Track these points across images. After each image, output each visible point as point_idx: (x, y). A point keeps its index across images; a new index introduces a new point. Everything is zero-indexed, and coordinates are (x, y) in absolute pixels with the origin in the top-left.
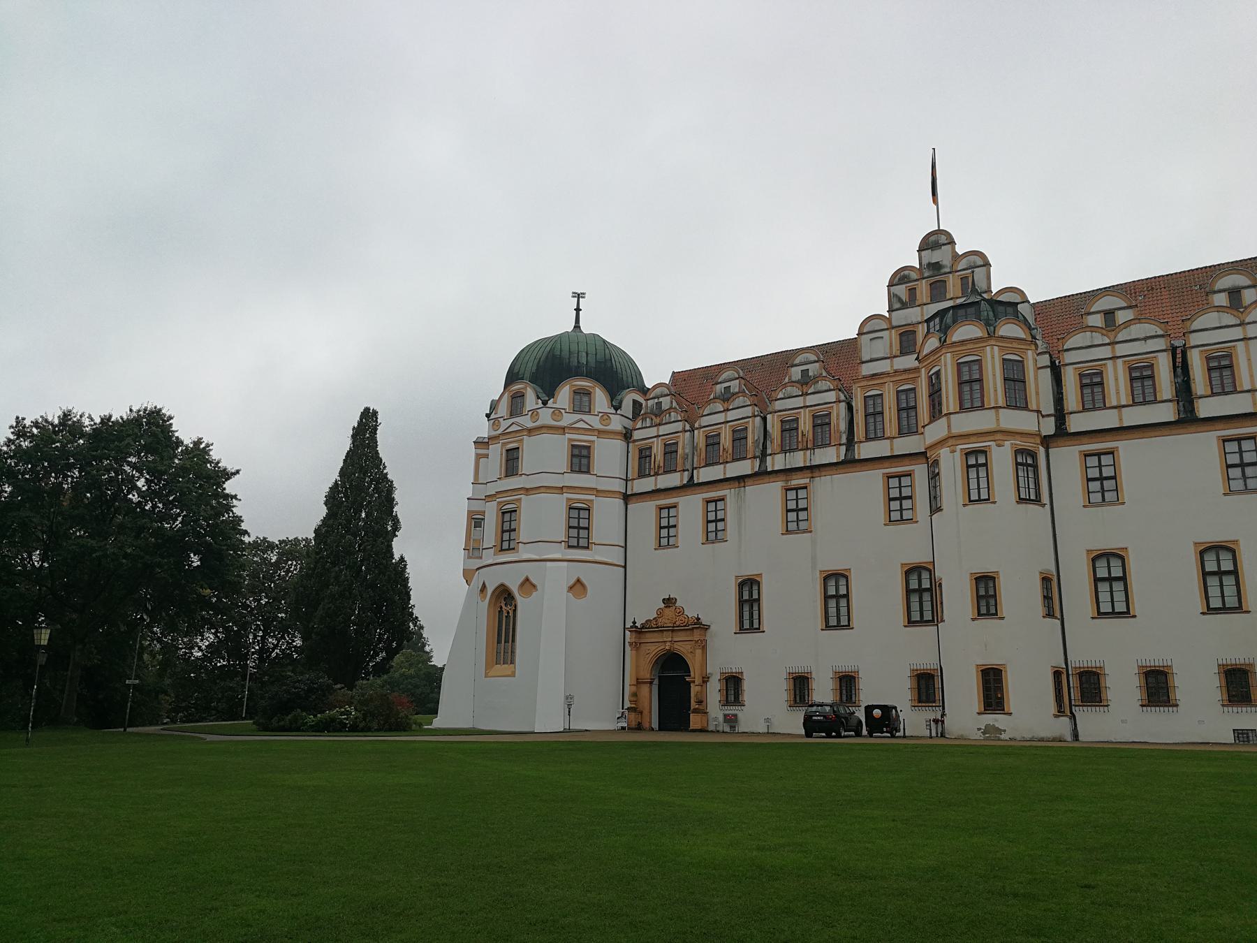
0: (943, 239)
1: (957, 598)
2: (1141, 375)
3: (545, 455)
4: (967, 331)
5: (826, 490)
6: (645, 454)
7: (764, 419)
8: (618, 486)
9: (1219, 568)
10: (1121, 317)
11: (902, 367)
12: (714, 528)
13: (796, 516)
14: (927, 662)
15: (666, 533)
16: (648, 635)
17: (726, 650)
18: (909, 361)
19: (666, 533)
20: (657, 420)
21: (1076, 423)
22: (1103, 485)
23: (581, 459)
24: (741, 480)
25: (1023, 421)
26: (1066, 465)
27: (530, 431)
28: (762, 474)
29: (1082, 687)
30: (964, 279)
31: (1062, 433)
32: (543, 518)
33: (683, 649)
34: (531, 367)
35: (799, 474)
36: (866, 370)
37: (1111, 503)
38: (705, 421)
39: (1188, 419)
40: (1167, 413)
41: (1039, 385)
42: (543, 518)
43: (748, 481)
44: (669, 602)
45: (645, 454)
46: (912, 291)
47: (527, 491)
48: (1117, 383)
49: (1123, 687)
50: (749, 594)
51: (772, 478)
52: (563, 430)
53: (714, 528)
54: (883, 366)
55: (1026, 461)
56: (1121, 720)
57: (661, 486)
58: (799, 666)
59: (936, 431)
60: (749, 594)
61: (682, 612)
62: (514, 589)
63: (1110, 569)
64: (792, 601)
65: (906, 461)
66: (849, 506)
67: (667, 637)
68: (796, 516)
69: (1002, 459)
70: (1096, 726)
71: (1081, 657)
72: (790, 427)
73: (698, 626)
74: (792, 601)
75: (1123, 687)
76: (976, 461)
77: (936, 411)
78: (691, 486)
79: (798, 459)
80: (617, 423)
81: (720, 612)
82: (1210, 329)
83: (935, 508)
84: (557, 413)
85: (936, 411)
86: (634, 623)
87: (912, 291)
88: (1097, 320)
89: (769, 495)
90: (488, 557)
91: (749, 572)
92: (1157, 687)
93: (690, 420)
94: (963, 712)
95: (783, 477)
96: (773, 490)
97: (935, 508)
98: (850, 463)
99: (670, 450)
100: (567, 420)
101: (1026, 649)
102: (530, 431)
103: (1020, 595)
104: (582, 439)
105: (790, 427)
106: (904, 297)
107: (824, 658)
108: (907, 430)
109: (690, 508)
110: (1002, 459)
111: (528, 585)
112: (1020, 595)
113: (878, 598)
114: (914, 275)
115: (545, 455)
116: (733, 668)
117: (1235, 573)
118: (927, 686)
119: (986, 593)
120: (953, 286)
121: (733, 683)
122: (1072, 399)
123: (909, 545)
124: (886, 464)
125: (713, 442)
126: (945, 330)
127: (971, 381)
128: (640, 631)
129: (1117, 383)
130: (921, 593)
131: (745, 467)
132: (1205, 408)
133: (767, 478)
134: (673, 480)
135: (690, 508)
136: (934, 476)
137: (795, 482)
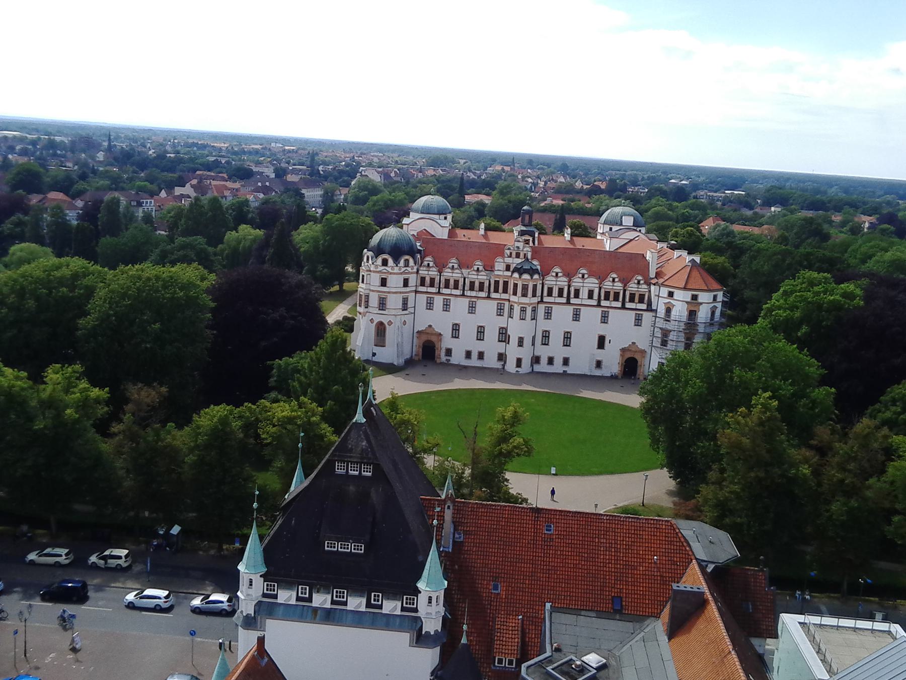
1: (514, 341)
2: (561, 291)
3: (395, 282)
4: (526, 276)
6: (423, 280)
8: (414, 289)
9: (567, 338)
10: (560, 274)
12: (446, 306)
13: (472, 309)
14: (503, 351)
15: (430, 305)
17: (448, 342)
18: (509, 273)
19: (430, 305)
21: (545, 299)
22: (548, 315)
23: (406, 283)
24: (456, 296)
25: (535, 300)
26: (541, 309)
27: (391, 273)
28: (463, 295)
29: (536, 360)
31: (542, 301)
32: (394, 302)
33: (434, 339)
34: (388, 249)
36: (496, 273)
39: (568, 303)
40: (564, 300)
41: (539, 287)
42: (394, 302)
44: (430, 326)
45: (423, 280)
47: (389, 292)
48: (555, 292)
49: (544, 360)
50: (456, 328)
52: (401, 274)
53: (446, 306)
54: (501, 273)
55: (534, 310)
56: (543, 367)
58: (469, 349)
59: (513, 298)
60: (456, 328)
62: (386, 323)
63: (546, 335)
66: (487, 308)
68: (472, 309)
69: (529, 310)
70: (537, 368)
71: (536, 354)
72: (472, 285)
75: (544, 360)
76: (523, 310)
77: (515, 293)
78: (439, 293)
80: (415, 270)
81: (447, 332)
82: (577, 282)
83: (510, 316)
84: (400, 269)
85: (515, 293)
88: (554, 274)
89: (465, 302)
90: (370, 309)
92: (551, 361)
93: (440, 272)
94: (511, 366)
96: (467, 300)
97: (510, 316)
98: (489, 297)
99: (432, 280)
100: (403, 269)
101: (526, 354)
102: (391, 273)
103: (527, 342)
104: (406, 276)
105: (472, 285)
107: (476, 347)
109: (438, 301)
110: (529, 310)
111: (390, 323)
112: (527, 342)
113: (492, 335)
115: (395, 282)
116: (449, 347)
118: (502, 357)
119: (521, 342)
120: (522, 256)
121: (449, 352)
122: (545, 293)
123: (502, 322)
125: (447, 282)
126: (521, 275)
127: (525, 288)
129: (555, 292)
130: (504, 335)
132: (573, 301)
135: (438, 301)
136: (511, 308)
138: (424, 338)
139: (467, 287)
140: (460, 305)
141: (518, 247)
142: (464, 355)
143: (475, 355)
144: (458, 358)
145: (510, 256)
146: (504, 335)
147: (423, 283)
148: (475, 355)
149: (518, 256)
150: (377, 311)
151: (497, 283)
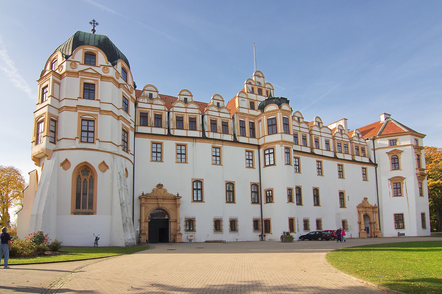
0: (261, 75)
5: (228, 151)
7: (203, 117)
11: (251, 114)
12: (182, 156)
13: (217, 158)
15: (157, 154)
16: (149, 200)
17: (188, 209)
19: (157, 154)
20: (151, 102)
28: (204, 138)
30: (267, 92)
33: (167, 206)
35: (219, 142)
37: (159, 161)
38: (175, 109)
43: (198, 140)
44: (160, 186)
46: (253, 88)
50: (198, 186)
51: (208, 141)
53: (182, 156)
57: (154, 132)
60: (198, 186)
61: (165, 191)
64: (214, 192)
65: (252, 146)
67: (161, 202)
68: (217, 158)
73: (176, 199)
74: (214, 192)
78: (169, 135)
79: (217, 136)
86: (143, 194)
87: (253, 88)
91: (198, 177)
95: (212, 142)
106: (251, 90)
108: (253, 135)
109: (170, 146)
113: (243, 193)
114: (253, 83)
116: (190, 216)
117: (201, 189)
120: (264, 93)
121: (191, 223)
124: (246, 146)
128: (144, 197)
131: (197, 134)
133: (206, 140)
134: (162, 131)
135: (170, 146)
137: (217, 145)
138: (151, 207)
139: (207, 127)
140: (200, 152)
141: (260, 83)
142: (211, 225)
143: (226, 225)
144: (204, 231)
145: (253, 92)
146: (259, 195)
147: (144, 118)
148: (226, 225)
149: (260, 92)
150: (77, 144)
151: (242, 123)
